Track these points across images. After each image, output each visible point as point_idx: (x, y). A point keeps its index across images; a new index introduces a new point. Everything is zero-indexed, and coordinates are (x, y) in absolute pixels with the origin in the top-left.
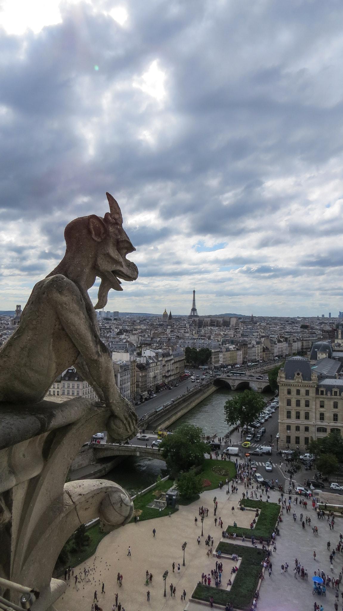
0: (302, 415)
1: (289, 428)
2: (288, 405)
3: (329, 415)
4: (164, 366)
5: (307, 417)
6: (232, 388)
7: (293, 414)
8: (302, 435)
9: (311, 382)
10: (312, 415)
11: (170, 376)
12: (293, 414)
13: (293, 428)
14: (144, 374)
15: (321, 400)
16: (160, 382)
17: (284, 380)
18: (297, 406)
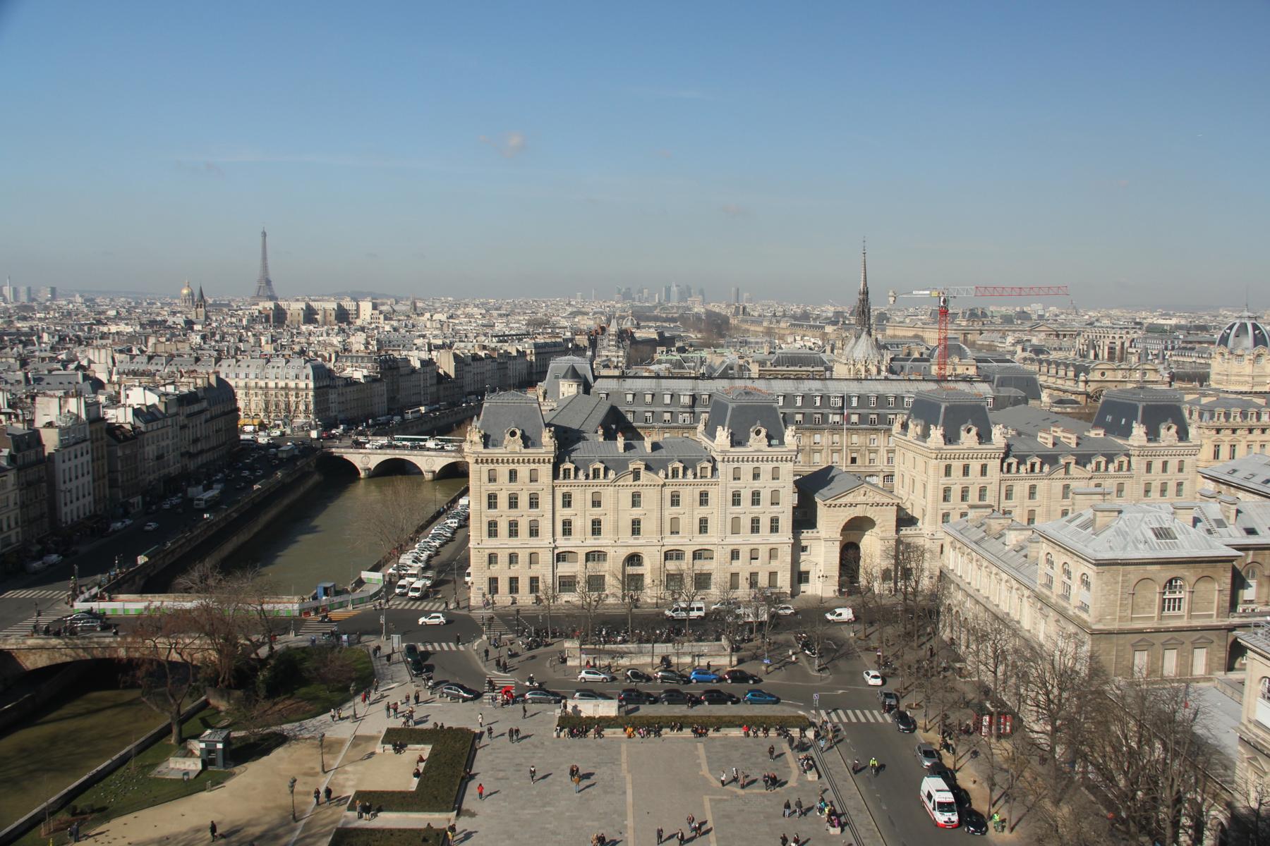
0: (523, 528)
1: (492, 559)
2: (490, 506)
3: (581, 524)
4: (183, 427)
5: (534, 532)
6: (362, 475)
7: (503, 528)
8: (523, 572)
9: (543, 450)
10: (545, 526)
11: (201, 452)
12: (503, 528)
13: (503, 558)
14: (128, 452)
15: (565, 490)
16: (174, 469)
17: (480, 448)
18: (510, 507)
